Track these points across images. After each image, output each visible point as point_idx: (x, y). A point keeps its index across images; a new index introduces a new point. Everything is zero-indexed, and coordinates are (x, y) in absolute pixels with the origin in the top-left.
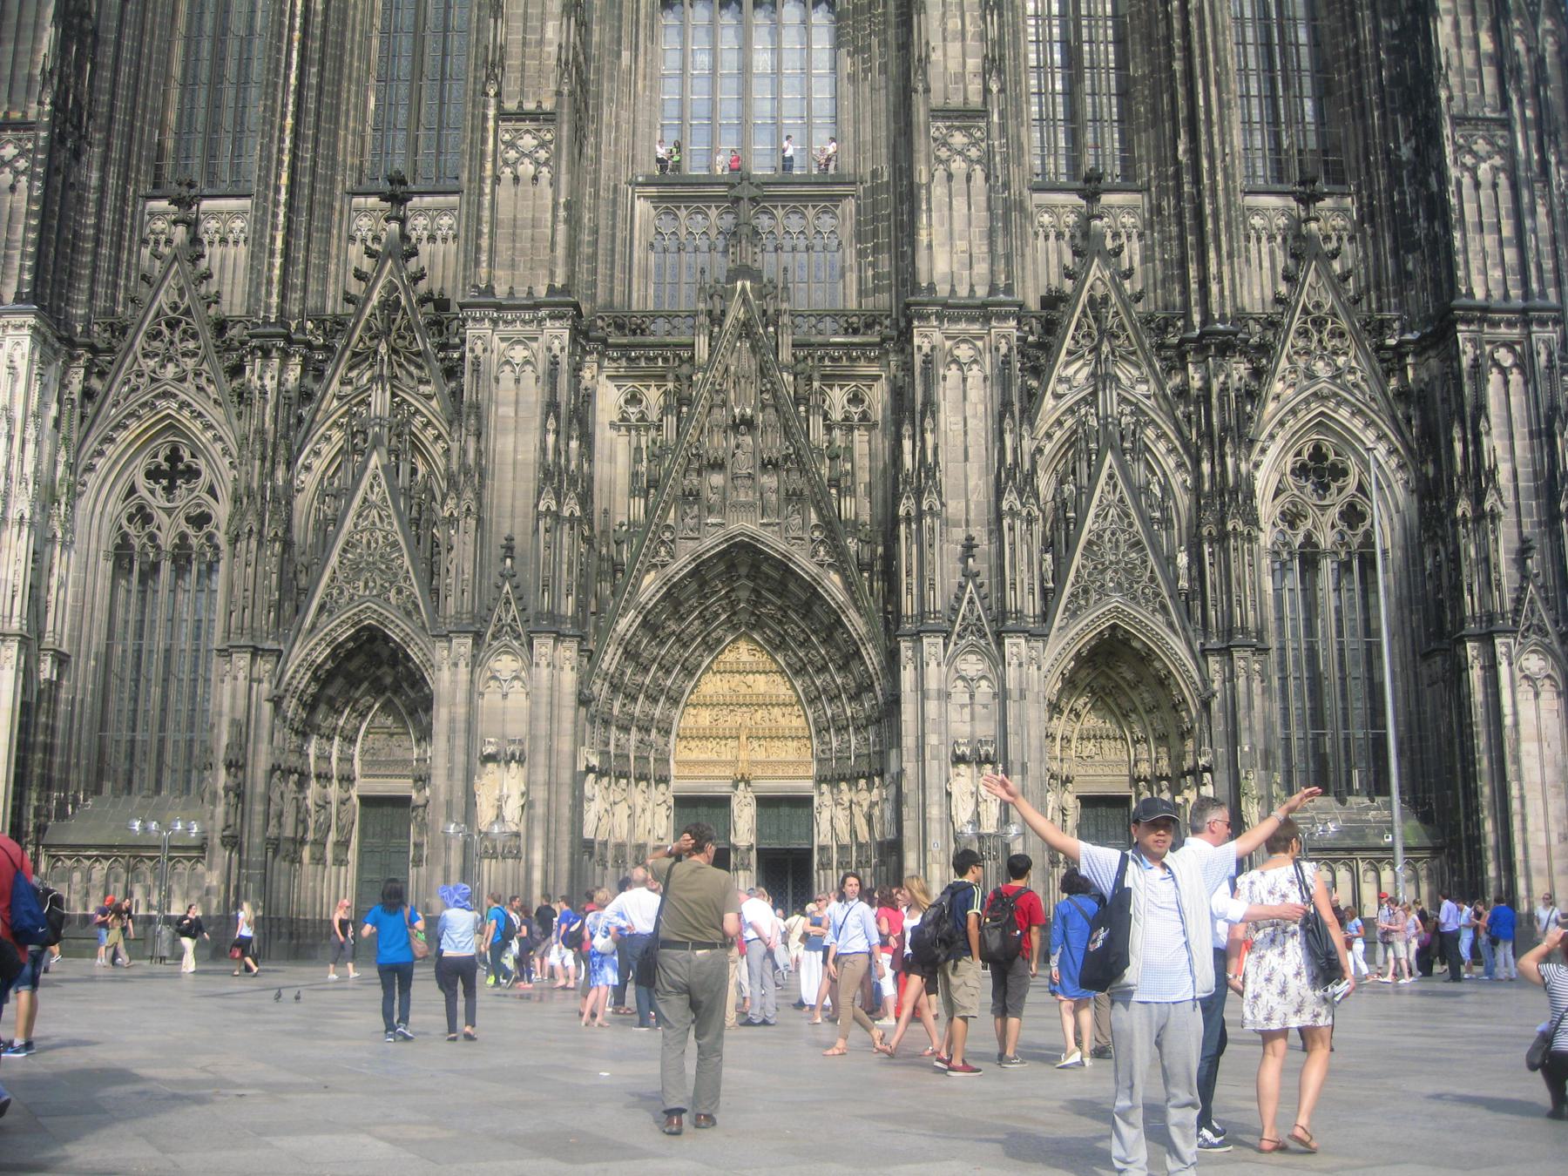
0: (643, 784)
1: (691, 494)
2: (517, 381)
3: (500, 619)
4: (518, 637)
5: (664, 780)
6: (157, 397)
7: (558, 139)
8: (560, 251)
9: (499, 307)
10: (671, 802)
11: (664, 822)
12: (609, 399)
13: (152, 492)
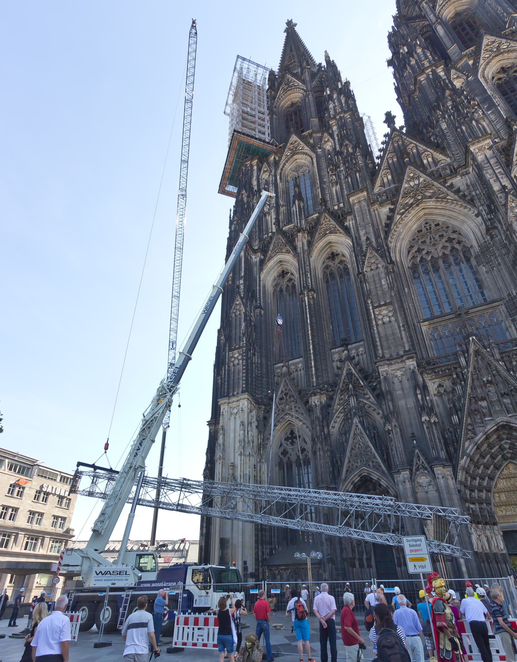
0: (488, 527)
1: (475, 410)
2: (401, 382)
3: (417, 464)
4: (426, 469)
5: (495, 524)
6: (285, 415)
7: (394, 309)
8: (405, 340)
9: (388, 360)
10: (502, 533)
11: (502, 543)
12: (432, 386)
13: (287, 445)
